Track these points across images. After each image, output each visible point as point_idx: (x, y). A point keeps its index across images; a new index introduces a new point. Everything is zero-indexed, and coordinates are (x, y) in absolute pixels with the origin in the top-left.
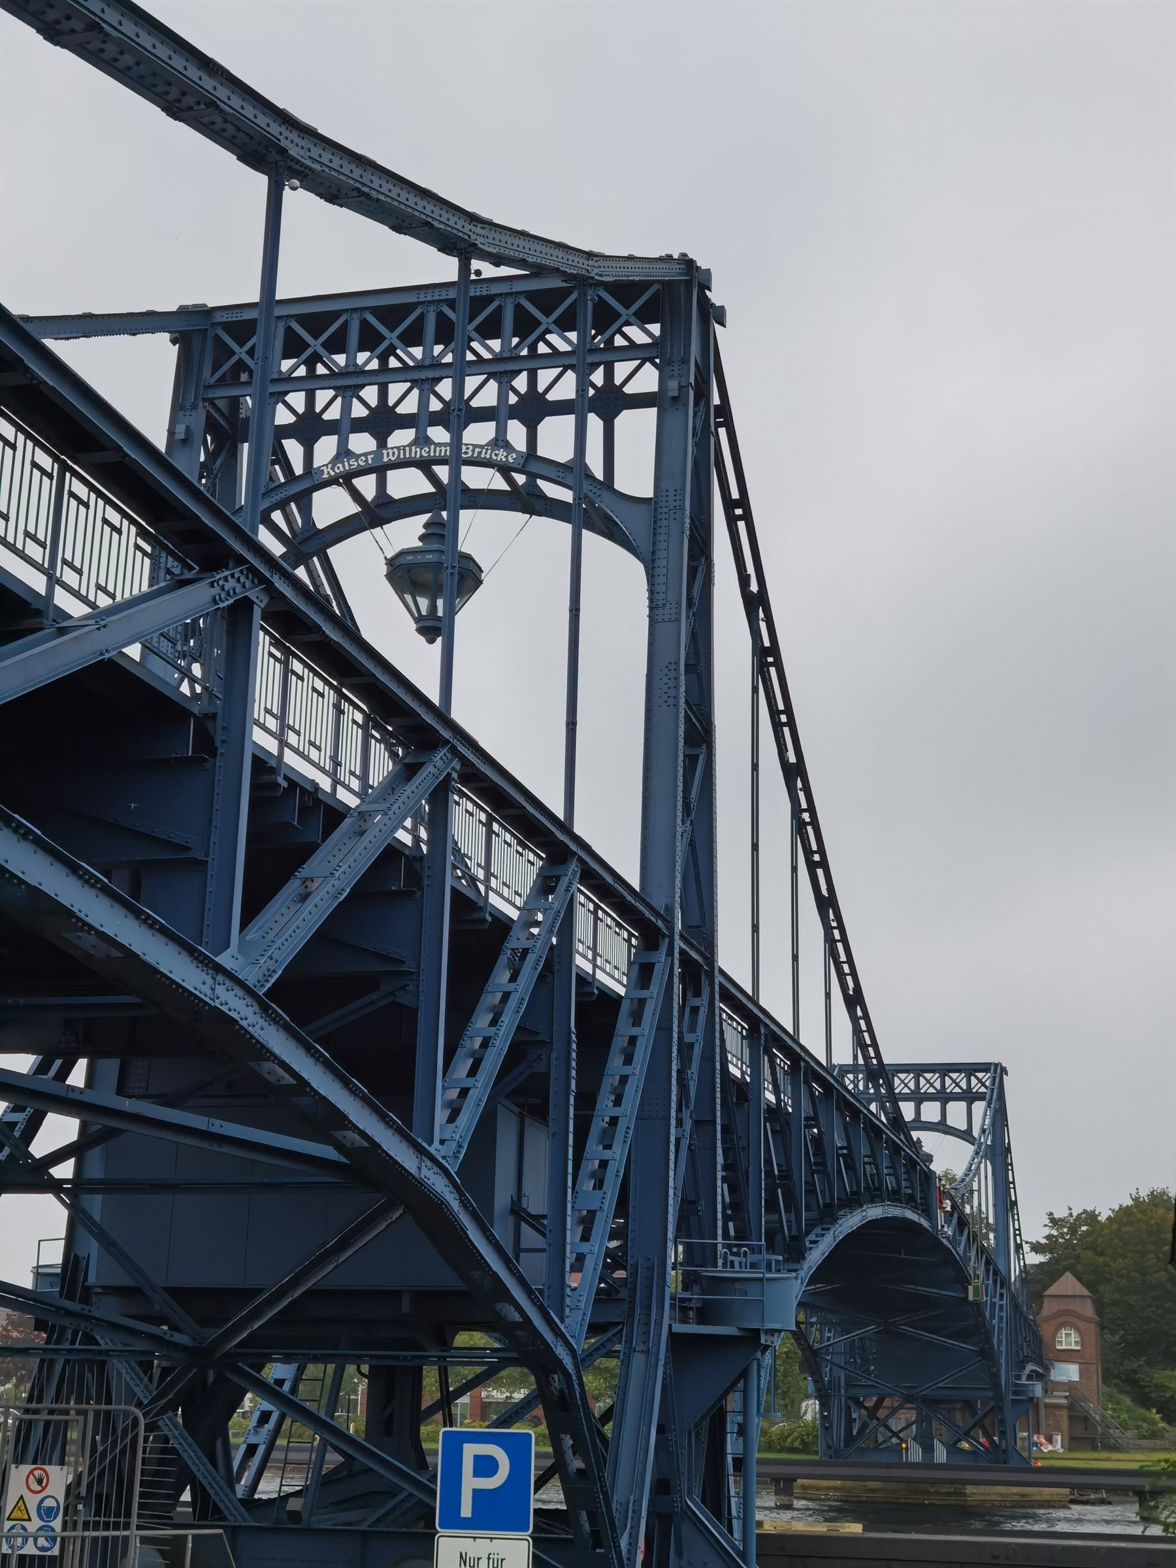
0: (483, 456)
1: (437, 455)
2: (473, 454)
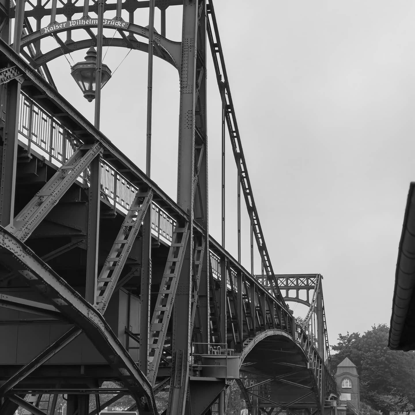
0: (111, 24)
1: (92, 23)
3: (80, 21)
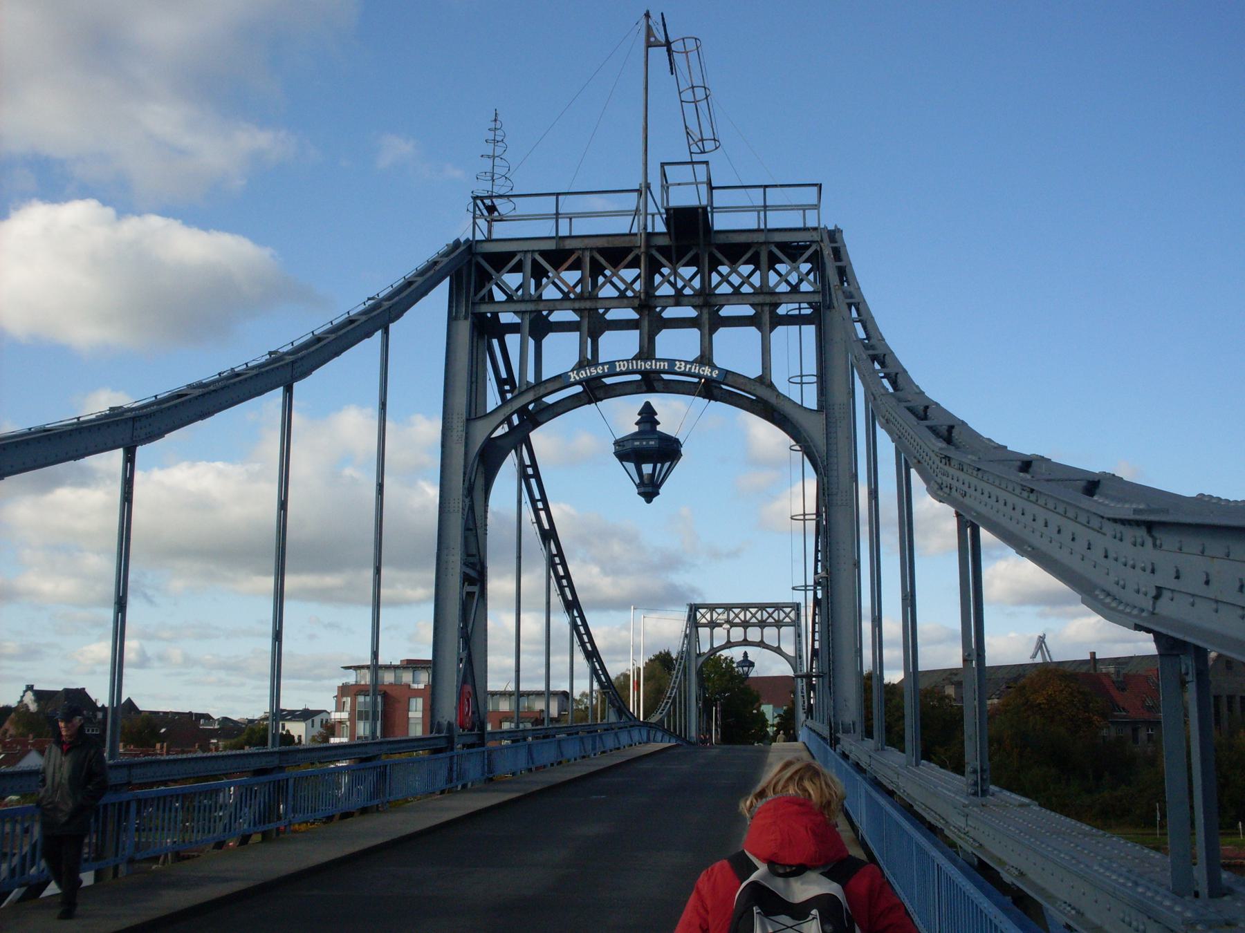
0: (693, 371)
1: (658, 368)
2: (685, 368)
3: (634, 362)
